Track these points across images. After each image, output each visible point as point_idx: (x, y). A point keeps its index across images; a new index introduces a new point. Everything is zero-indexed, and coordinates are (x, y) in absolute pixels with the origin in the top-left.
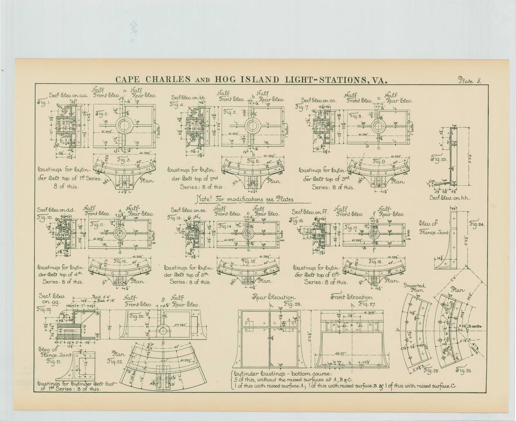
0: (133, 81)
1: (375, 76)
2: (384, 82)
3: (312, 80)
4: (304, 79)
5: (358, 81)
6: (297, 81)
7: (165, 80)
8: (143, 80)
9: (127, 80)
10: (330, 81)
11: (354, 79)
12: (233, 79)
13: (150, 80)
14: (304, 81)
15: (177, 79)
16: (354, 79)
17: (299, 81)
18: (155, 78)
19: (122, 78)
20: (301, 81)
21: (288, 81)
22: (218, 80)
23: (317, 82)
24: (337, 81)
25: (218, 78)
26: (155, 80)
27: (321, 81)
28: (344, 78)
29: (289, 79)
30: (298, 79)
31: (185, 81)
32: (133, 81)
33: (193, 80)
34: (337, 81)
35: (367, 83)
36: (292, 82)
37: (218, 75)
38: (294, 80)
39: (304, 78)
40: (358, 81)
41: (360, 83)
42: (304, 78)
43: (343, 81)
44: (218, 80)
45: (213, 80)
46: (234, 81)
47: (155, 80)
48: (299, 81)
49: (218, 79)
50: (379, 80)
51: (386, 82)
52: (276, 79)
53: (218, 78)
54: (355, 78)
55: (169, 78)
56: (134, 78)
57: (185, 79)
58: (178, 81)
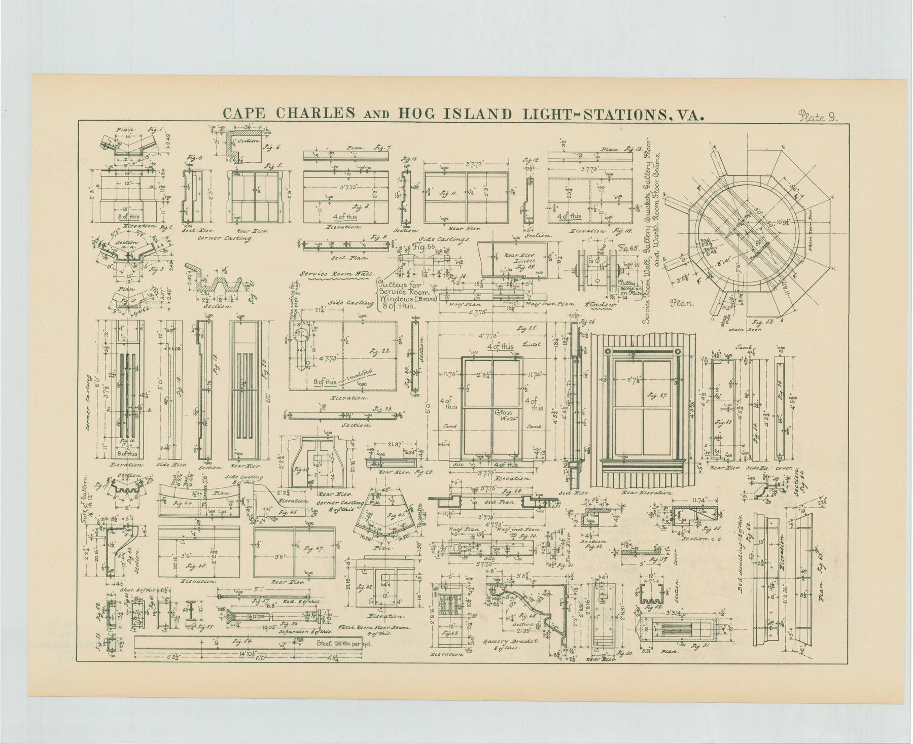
0: (253, 116)
1: (683, 108)
2: (698, 118)
3: (571, 115)
4: (556, 113)
5: (652, 117)
6: (545, 117)
7: (310, 114)
8: (270, 114)
9: (244, 115)
10: (603, 116)
11: (644, 113)
12: (430, 113)
13: (285, 114)
14: (556, 117)
15: (331, 112)
16: (644, 113)
17: (548, 117)
18: (293, 112)
19: (234, 111)
20: (551, 117)
21: (528, 117)
22: (404, 115)
23: (580, 119)
24: (616, 116)
25: (404, 111)
26: (293, 115)
27: (587, 116)
28: (627, 112)
29: (531, 113)
30: (545, 113)
31: (345, 116)
32: (253, 116)
33: (360, 114)
34: (616, 116)
35: (668, 120)
36: (536, 118)
37: (404, 106)
38: (539, 116)
39: (556, 112)
40: (652, 117)
41: (656, 117)
42: (556, 112)
43: (625, 116)
44: (404, 115)
45: (395, 115)
46: (433, 116)
47: (293, 115)
48: (548, 117)
49: (404, 113)
50: (689, 114)
51: (702, 119)
52: (507, 114)
53: (404, 111)
54: (648, 111)
55: (316, 110)
56: (255, 110)
57: (345, 112)
58: (334, 115)
